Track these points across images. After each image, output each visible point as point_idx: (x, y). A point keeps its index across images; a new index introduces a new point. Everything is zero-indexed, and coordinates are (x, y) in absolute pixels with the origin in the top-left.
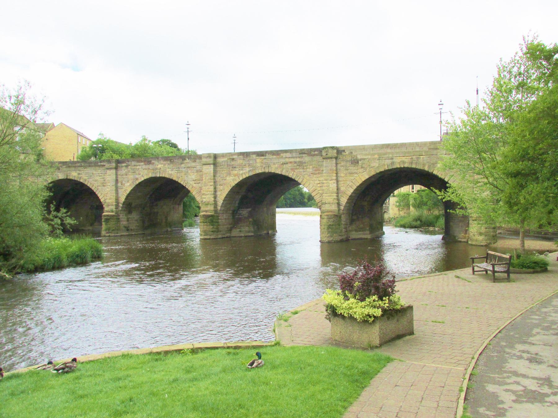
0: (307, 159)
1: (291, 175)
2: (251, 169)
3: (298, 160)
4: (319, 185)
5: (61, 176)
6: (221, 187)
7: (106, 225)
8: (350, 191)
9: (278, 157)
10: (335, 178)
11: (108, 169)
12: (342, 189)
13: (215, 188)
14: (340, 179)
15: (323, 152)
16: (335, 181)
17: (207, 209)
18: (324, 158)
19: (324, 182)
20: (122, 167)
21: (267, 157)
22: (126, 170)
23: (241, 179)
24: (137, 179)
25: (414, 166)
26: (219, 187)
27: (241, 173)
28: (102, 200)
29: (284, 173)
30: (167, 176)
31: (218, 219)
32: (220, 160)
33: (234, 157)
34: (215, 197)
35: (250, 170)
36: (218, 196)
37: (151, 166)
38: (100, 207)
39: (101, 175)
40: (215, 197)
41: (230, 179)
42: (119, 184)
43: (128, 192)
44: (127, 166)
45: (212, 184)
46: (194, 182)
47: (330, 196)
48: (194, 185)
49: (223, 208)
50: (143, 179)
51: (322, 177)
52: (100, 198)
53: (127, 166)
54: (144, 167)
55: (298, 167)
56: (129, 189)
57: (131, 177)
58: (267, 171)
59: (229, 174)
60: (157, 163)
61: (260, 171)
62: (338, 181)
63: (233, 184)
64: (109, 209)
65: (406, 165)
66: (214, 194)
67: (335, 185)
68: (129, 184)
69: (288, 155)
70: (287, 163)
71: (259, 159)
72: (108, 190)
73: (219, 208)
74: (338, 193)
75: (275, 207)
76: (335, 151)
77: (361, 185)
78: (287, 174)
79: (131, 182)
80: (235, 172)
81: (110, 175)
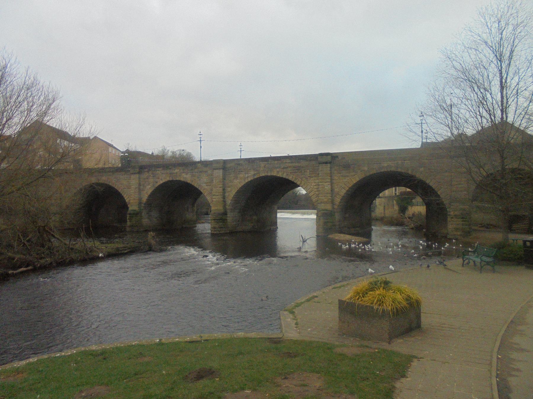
0: (303, 163)
1: (291, 177)
2: (255, 172)
3: (297, 164)
4: (315, 187)
5: (94, 180)
6: (229, 189)
7: (130, 221)
8: (343, 192)
9: (279, 162)
10: (329, 180)
11: (132, 174)
12: (336, 190)
13: (224, 190)
15: (319, 157)
16: (329, 183)
17: (216, 208)
18: (319, 163)
19: (320, 184)
21: (269, 162)
22: (147, 174)
23: (246, 181)
24: (157, 182)
25: (399, 170)
27: (246, 176)
28: (127, 201)
29: (284, 176)
30: (182, 179)
33: (240, 162)
34: (224, 197)
35: (255, 174)
37: (168, 171)
38: (124, 206)
39: (126, 179)
40: (224, 197)
41: (236, 182)
42: (142, 187)
43: (149, 193)
44: (148, 172)
46: (205, 184)
47: (325, 196)
48: (206, 187)
50: (161, 182)
51: (318, 179)
52: (125, 198)
53: (148, 172)
54: (163, 172)
55: (297, 171)
56: (150, 192)
57: (151, 180)
58: (269, 174)
59: (236, 178)
60: (174, 168)
61: (264, 175)
62: (332, 184)
63: (240, 186)
64: (133, 207)
65: (393, 169)
67: (330, 187)
68: (149, 186)
69: (288, 161)
70: (287, 168)
71: (262, 164)
72: (132, 192)
73: (227, 207)
74: (332, 194)
75: (276, 207)
76: (329, 157)
77: (353, 186)
78: (287, 177)
79: (151, 184)
80: (241, 176)
81: (134, 180)
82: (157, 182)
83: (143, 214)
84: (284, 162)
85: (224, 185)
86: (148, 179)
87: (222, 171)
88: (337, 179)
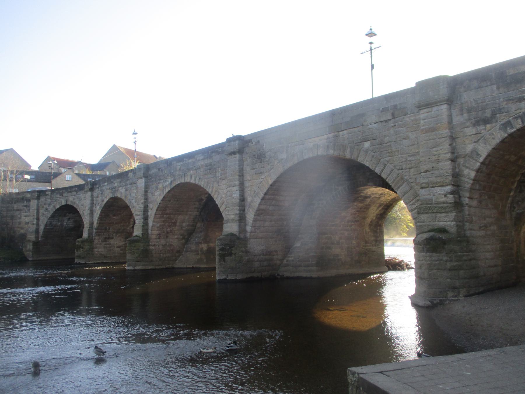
1: (203, 183)
2: (172, 179)
10: (237, 183)
12: (249, 199)
14: (247, 184)
16: (237, 188)
20: (96, 188)
26: (151, 206)
31: (149, 245)
32: (153, 171)
36: (149, 216)
44: (98, 188)
45: (143, 201)
49: (156, 232)
61: (179, 182)
66: (144, 214)
82: (103, 201)
83: (96, 242)
84: (198, 159)
85: (146, 199)
86: (98, 197)
87: (144, 181)
88: (250, 180)
